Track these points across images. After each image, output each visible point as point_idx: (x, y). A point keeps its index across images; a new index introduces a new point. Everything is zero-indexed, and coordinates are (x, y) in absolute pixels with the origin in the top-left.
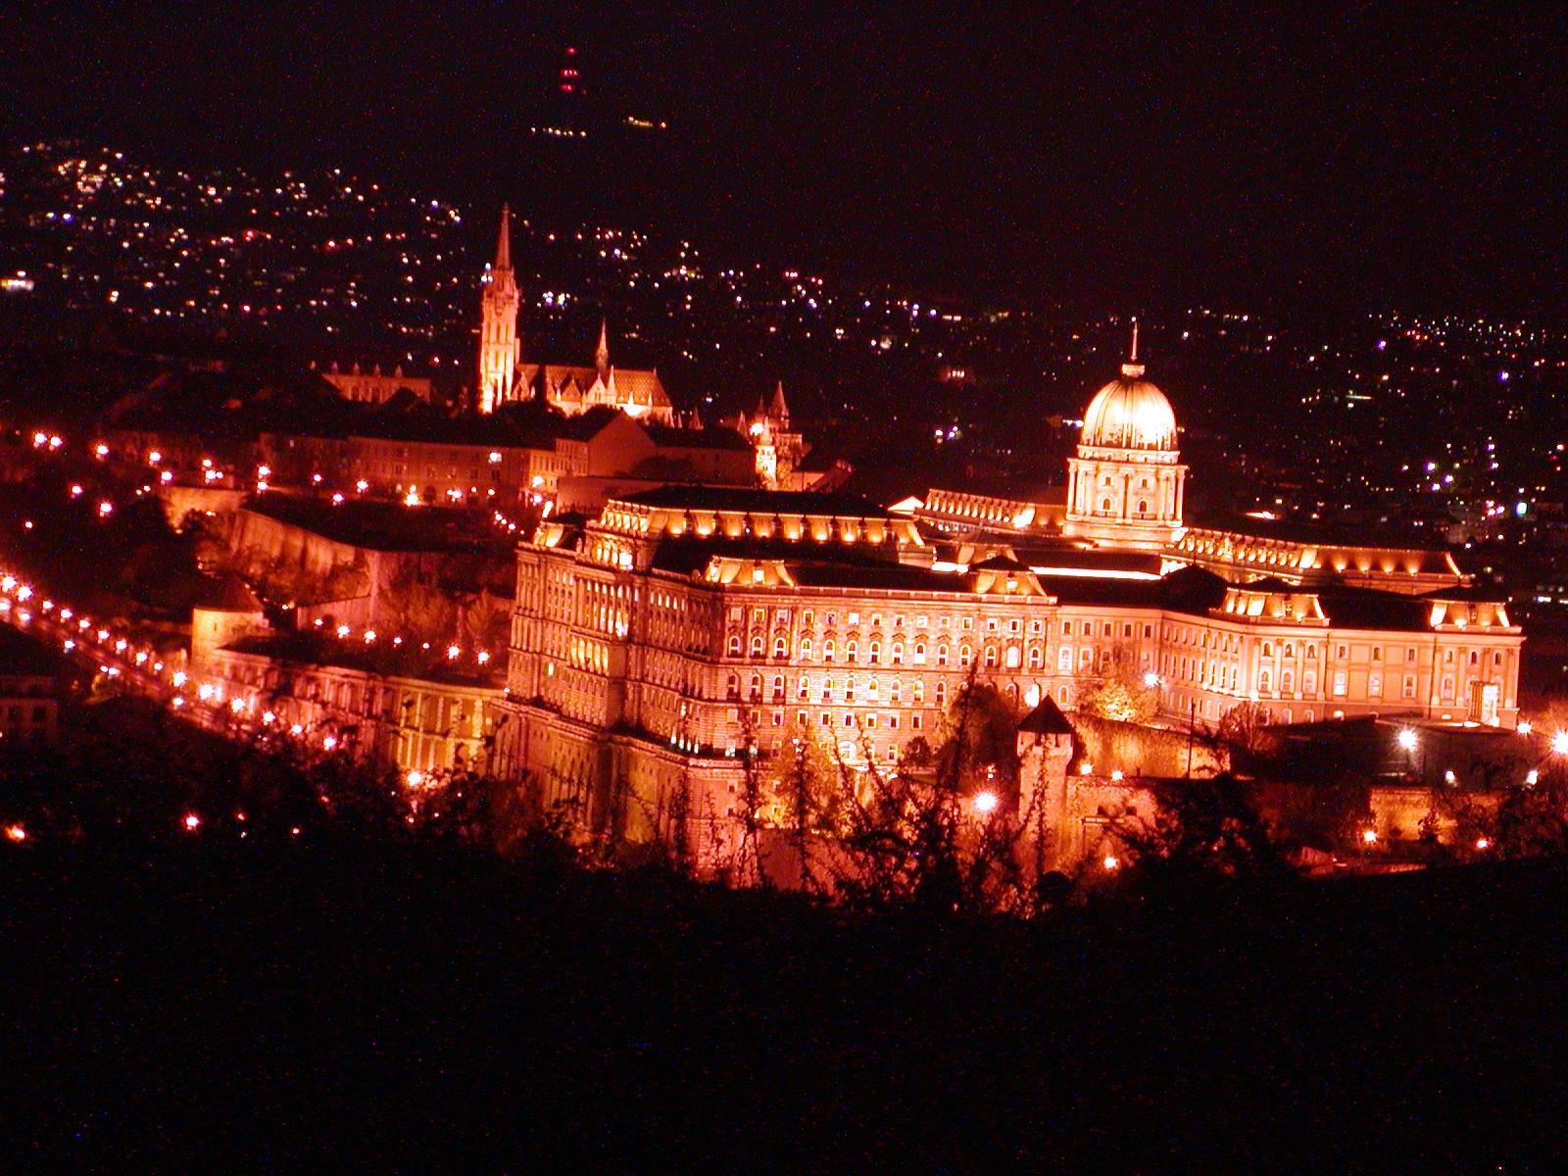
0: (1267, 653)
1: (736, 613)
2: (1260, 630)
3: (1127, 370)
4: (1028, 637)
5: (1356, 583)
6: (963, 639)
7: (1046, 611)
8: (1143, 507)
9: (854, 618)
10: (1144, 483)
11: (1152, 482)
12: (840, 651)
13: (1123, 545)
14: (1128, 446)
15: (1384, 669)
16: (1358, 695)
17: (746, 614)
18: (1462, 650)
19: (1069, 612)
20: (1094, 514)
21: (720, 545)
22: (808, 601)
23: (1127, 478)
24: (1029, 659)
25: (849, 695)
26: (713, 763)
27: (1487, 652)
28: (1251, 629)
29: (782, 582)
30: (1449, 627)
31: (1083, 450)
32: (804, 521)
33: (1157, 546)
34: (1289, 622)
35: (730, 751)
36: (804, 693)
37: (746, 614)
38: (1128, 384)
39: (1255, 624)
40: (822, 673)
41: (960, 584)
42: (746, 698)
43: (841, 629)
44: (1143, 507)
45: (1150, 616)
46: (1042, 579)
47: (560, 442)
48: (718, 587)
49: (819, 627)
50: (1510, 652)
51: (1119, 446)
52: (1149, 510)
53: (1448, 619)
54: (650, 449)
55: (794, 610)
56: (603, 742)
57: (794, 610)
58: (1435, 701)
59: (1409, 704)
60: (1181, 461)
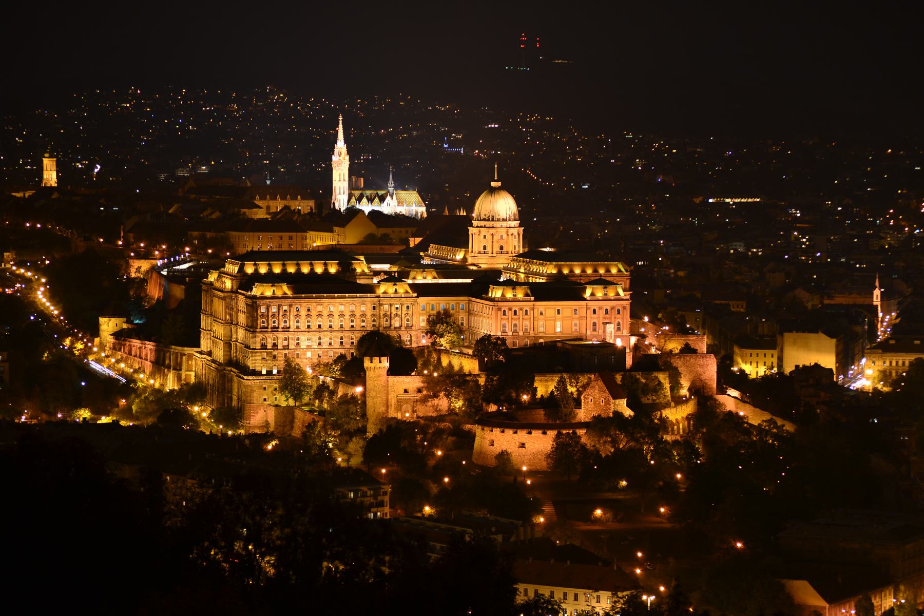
0: (504, 314)
1: (263, 309)
2: (500, 304)
3: (493, 184)
4: (404, 312)
5: (573, 279)
6: (373, 315)
7: (411, 300)
8: (501, 248)
9: (320, 308)
10: (502, 237)
11: (505, 236)
12: (314, 324)
13: (492, 266)
14: (493, 220)
15: (562, 319)
16: (550, 331)
17: (268, 309)
18: (600, 308)
19: (423, 300)
20: (479, 253)
21: (257, 278)
22: (297, 301)
23: (492, 235)
24: (405, 323)
25: (320, 344)
26: (254, 378)
27: (612, 308)
28: (496, 304)
29: (285, 293)
30: (593, 298)
31: (475, 223)
32: (255, 264)
33: (502, 266)
34: (515, 299)
35: (264, 372)
36: (298, 344)
37: (268, 309)
38: (493, 191)
39: (498, 301)
40: (306, 334)
41: (370, 289)
42: (269, 347)
43: (314, 313)
44: (501, 248)
45: (463, 300)
46: (409, 285)
47: (335, 228)
48: (254, 297)
49: (303, 313)
50: (624, 308)
51: (488, 220)
52: (504, 249)
53: (592, 294)
54: (372, 228)
55: (290, 306)
56: (221, 370)
57: (290, 306)
58: (588, 333)
59: (576, 334)
60: (520, 226)
